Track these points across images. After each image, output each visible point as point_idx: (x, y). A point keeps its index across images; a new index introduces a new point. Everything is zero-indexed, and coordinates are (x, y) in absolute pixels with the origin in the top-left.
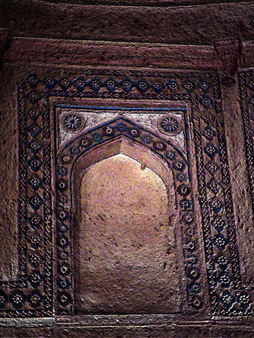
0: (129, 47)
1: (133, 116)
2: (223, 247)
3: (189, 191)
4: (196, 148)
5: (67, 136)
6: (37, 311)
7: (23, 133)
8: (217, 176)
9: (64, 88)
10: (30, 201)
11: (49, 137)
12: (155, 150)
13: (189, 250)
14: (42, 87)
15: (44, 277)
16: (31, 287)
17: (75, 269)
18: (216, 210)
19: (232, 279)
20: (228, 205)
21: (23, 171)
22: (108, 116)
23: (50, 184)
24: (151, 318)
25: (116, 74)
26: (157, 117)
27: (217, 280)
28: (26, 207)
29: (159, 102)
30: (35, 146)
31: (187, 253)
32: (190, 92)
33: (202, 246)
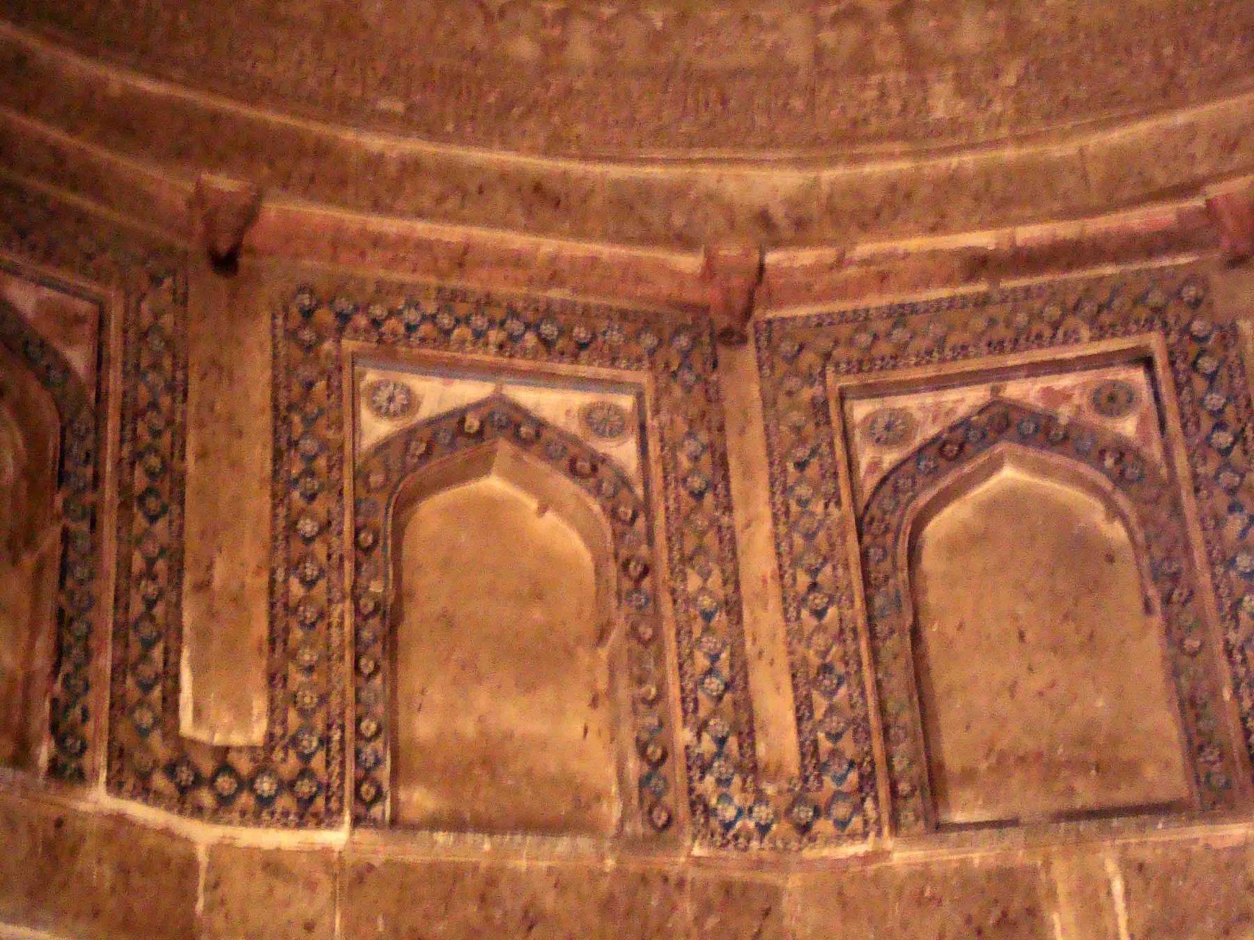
0: (518, 241)
1: (527, 396)
2: (719, 698)
3: (646, 571)
4: (665, 478)
5: (375, 429)
6: (307, 813)
7: (280, 416)
8: (711, 539)
9: (376, 323)
10: (293, 566)
11: (340, 428)
12: (573, 471)
13: (644, 701)
14: (325, 316)
15: (325, 741)
16: (293, 759)
17: (389, 729)
18: (707, 616)
19: (739, 768)
20: (733, 607)
21: (278, 499)
22: (469, 391)
23: (340, 533)
24: (563, 845)
25: (487, 301)
26: (579, 399)
27: (705, 769)
28: (286, 581)
29: (584, 370)
30: (309, 445)
31: (642, 708)
32: (652, 352)
33: (674, 692)
